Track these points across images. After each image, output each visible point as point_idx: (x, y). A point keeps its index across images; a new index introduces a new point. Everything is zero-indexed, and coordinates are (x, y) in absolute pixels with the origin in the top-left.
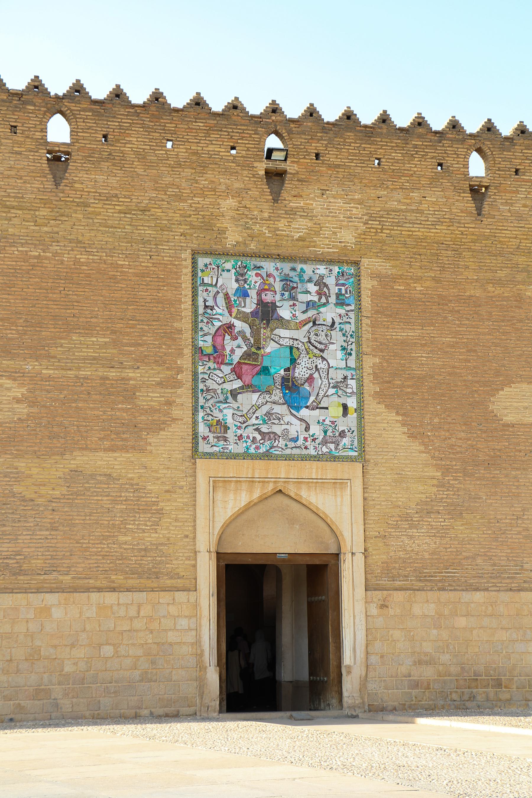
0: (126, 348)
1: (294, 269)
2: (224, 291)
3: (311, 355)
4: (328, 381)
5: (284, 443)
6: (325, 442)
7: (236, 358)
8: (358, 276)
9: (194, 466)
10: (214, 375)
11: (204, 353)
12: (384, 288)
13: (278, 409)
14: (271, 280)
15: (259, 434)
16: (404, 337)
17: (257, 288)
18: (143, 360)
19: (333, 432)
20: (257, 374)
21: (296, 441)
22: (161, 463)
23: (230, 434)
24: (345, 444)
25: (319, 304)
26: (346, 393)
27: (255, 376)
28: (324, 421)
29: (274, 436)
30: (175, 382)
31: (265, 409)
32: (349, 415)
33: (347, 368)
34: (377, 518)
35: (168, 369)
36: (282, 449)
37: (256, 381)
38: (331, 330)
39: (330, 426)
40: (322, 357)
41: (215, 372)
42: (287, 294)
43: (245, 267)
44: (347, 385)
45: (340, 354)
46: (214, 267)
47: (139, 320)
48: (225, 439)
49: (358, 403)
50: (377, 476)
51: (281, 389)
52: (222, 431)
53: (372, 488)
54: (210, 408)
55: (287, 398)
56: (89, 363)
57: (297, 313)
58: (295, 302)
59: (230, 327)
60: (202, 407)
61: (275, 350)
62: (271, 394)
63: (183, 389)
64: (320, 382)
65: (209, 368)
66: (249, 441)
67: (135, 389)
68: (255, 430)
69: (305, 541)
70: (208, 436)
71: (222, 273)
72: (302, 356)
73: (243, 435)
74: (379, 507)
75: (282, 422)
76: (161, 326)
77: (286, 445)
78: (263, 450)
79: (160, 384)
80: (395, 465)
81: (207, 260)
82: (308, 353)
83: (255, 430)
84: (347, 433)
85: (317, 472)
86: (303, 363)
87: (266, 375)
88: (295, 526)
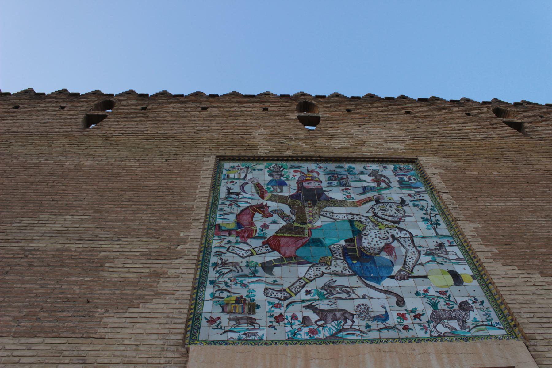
2: (256, 182)
5: (364, 323)
6: (437, 318)
7: (271, 232)
9: (184, 359)
10: (235, 249)
11: (223, 228)
16: (503, 207)
17: (297, 179)
20: (302, 246)
23: (260, 315)
24: (475, 320)
25: (379, 188)
26: (450, 260)
27: (300, 249)
28: (426, 291)
29: (343, 315)
30: (171, 253)
31: (321, 282)
35: (163, 241)
36: (361, 332)
37: (302, 252)
38: (402, 206)
40: (399, 228)
41: (237, 246)
42: (335, 183)
47: (137, 202)
48: (251, 322)
49: (473, 270)
51: (345, 259)
52: (246, 310)
54: (226, 283)
56: (49, 236)
57: (352, 195)
58: (347, 188)
59: (261, 209)
60: (212, 282)
62: (329, 266)
63: (182, 260)
64: (404, 251)
65: (229, 242)
67: (107, 259)
70: (219, 318)
71: (254, 172)
72: (368, 227)
73: (286, 314)
75: (353, 296)
76: (166, 205)
77: (368, 326)
78: (323, 334)
79: (148, 256)
81: (235, 164)
83: (307, 307)
84: (473, 305)
87: (318, 246)
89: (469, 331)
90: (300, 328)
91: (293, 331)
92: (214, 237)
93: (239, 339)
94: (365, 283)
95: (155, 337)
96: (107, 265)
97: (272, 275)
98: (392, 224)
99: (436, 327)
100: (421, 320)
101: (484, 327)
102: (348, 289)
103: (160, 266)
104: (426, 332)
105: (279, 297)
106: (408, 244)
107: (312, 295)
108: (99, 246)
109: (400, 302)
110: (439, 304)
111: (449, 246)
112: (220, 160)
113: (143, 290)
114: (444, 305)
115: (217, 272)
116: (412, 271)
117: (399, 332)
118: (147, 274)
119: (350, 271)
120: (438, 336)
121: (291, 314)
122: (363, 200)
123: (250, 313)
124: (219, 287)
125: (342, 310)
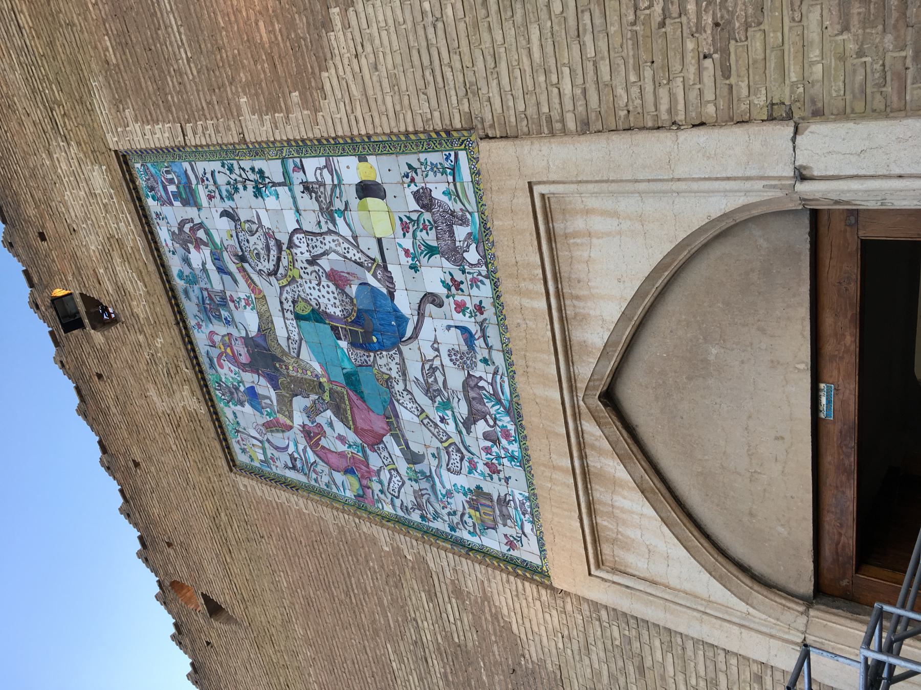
0: (392, 626)
1: (186, 292)
3: (295, 273)
4: (325, 233)
5: (481, 366)
7: (352, 437)
8: (142, 153)
12: (127, 91)
13: (414, 370)
14: (217, 339)
15: (475, 422)
17: (237, 369)
18: (402, 607)
19: (425, 228)
20: (364, 402)
21: (470, 333)
22: (577, 658)
26: (334, 186)
28: (407, 252)
29: (472, 388)
32: (379, 180)
33: (287, 182)
34: (648, 73)
36: (495, 373)
37: (376, 404)
39: (414, 237)
43: (220, 385)
44: (318, 182)
45: (271, 202)
46: (239, 438)
48: (503, 502)
50: (505, 81)
53: (543, 98)
55: (387, 343)
57: (242, 296)
59: (307, 433)
61: (313, 352)
62: (390, 377)
64: (333, 256)
66: (495, 449)
68: (469, 432)
69: (762, 330)
70: (506, 536)
74: (604, 68)
80: (460, 14)
81: (236, 448)
82: (293, 280)
83: (469, 432)
85: (528, 294)
86: (315, 294)
88: (712, 358)
89: (469, 213)
90: (503, 448)
91: (510, 459)
92: (378, 507)
93: (533, 522)
94: (410, 338)
95: (547, 616)
96: (456, 640)
97: (424, 455)
98: (283, 253)
99: (472, 265)
100: (462, 283)
101: (458, 185)
102: (427, 367)
103: (443, 586)
104: (483, 283)
105: (458, 458)
106: (318, 244)
107: (446, 417)
108: (430, 643)
109: (434, 300)
110: (426, 241)
111: (304, 172)
112: (235, 465)
113: (484, 612)
114: (428, 233)
115: (434, 519)
116: (374, 260)
117: (487, 322)
118: (460, 603)
119: (394, 351)
120: (487, 267)
121: (484, 454)
122: (247, 282)
123: (492, 501)
124: (457, 523)
125: (465, 385)
